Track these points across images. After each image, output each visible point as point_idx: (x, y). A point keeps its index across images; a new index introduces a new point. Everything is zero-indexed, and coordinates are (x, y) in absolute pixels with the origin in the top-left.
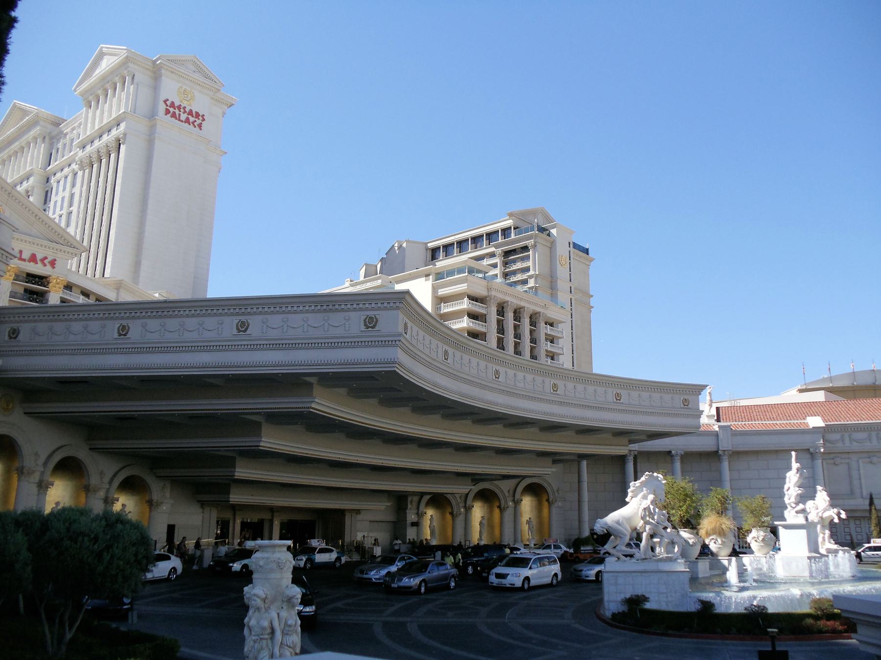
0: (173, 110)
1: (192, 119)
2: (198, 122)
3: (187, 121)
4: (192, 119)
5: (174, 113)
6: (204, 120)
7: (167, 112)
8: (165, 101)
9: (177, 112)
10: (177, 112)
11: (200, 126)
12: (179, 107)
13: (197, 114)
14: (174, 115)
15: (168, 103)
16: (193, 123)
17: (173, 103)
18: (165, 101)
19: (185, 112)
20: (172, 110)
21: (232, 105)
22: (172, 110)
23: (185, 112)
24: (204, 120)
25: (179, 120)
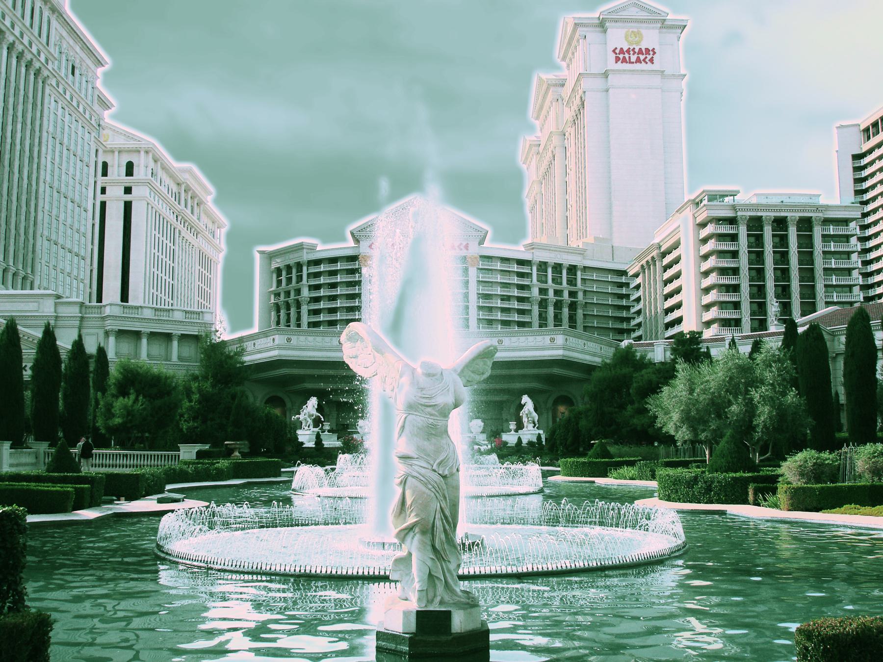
0: (621, 56)
1: (642, 57)
2: (649, 57)
3: (638, 60)
4: (642, 57)
5: (624, 58)
6: (654, 53)
7: (617, 59)
8: (614, 51)
9: (627, 56)
10: (627, 56)
11: (651, 60)
12: (628, 51)
13: (647, 50)
14: (624, 60)
15: (617, 51)
16: (644, 60)
17: (622, 49)
18: (614, 51)
19: (634, 53)
20: (621, 56)
21: (685, 26)
22: (621, 56)
23: (634, 53)
24: (654, 53)
25: (630, 62)
